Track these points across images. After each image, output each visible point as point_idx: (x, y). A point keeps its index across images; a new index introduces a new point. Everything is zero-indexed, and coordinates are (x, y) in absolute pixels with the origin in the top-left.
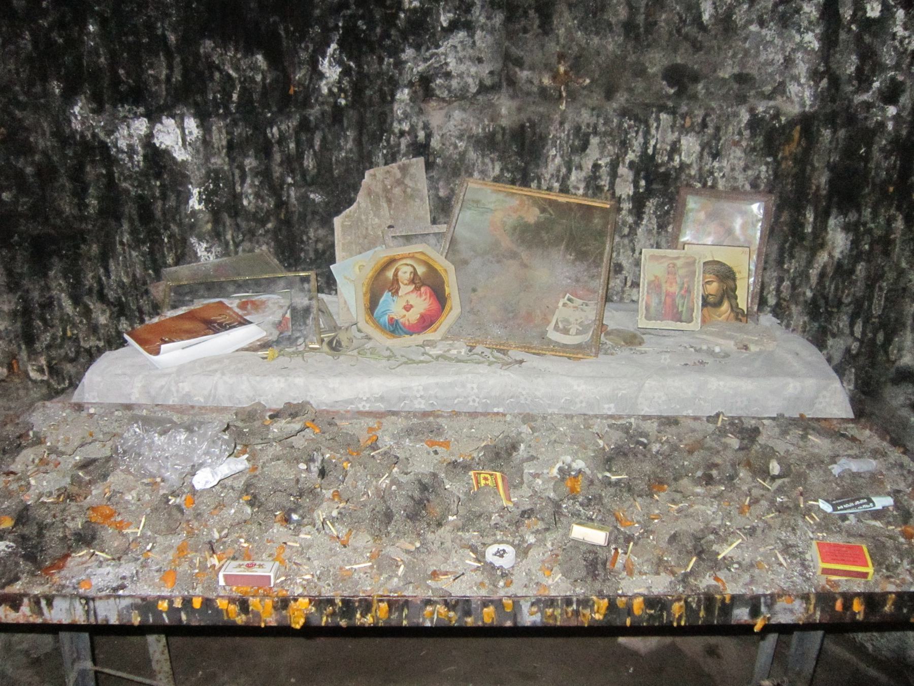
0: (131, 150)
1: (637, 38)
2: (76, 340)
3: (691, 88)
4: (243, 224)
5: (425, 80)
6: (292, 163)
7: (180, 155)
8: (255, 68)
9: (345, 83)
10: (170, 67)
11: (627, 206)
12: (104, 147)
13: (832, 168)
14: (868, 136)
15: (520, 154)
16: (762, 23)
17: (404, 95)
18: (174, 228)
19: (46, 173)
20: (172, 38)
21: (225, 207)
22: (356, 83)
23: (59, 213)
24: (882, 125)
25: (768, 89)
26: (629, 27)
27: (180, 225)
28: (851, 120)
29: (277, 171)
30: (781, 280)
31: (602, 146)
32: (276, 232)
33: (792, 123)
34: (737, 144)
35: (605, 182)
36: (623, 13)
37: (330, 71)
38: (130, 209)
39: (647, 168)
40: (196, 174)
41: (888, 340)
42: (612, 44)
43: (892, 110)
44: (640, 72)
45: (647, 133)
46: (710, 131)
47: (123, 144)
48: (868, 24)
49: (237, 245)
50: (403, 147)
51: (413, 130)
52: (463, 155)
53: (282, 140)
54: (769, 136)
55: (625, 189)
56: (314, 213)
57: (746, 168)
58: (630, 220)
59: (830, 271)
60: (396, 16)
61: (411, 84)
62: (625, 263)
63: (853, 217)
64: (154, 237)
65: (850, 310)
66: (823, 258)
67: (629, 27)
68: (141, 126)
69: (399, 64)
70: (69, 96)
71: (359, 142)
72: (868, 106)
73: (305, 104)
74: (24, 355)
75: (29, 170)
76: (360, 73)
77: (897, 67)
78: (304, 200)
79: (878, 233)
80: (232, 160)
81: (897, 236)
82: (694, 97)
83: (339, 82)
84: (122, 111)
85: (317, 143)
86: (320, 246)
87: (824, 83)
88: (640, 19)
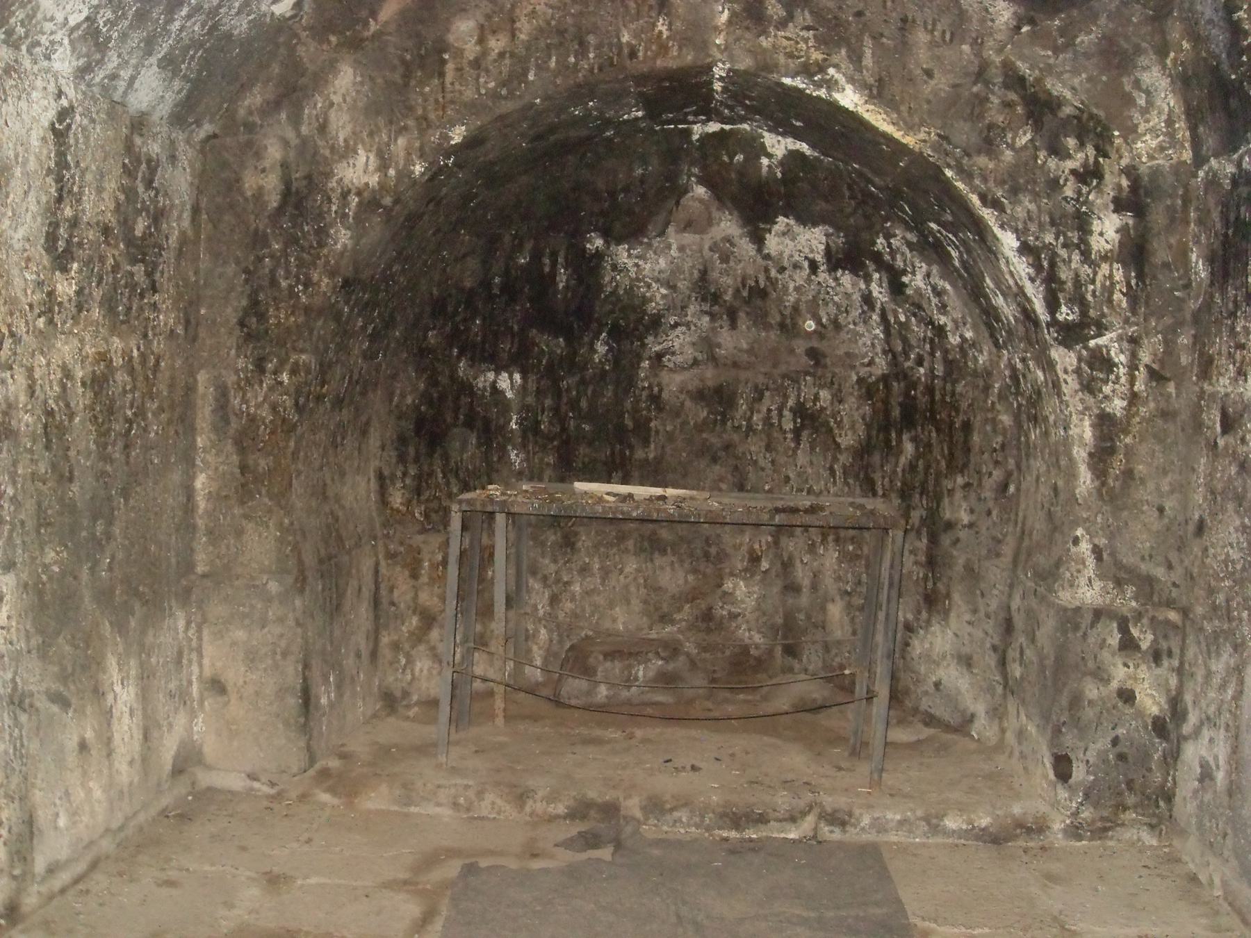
0: (485, 388)
1: (787, 331)
2: (439, 499)
3: (823, 361)
4: (540, 440)
5: (659, 356)
6: (574, 405)
7: (509, 395)
8: (558, 345)
9: (610, 356)
10: (512, 343)
11: (789, 436)
12: (471, 386)
13: (900, 404)
14: (913, 385)
15: (720, 403)
16: (855, 324)
17: (646, 364)
18: (500, 439)
19: (442, 398)
20: (516, 327)
21: (531, 429)
22: (616, 358)
23: (445, 421)
24: (919, 378)
25: (866, 360)
26: (782, 326)
27: (504, 437)
28: (906, 376)
29: (564, 408)
30: (883, 478)
31: (772, 396)
32: (558, 449)
33: (878, 381)
34: (852, 394)
35: (775, 421)
36: (778, 318)
37: (601, 348)
38: (479, 424)
39: (800, 410)
40: (515, 406)
41: (938, 506)
42: (773, 335)
43: (922, 370)
44: (792, 351)
45: (799, 389)
46: (836, 386)
47: (480, 385)
48: (900, 324)
49: (534, 454)
50: (644, 397)
51: (650, 387)
52: (683, 404)
53: (568, 390)
54: (868, 390)
55: (788, 425)
56: (584, 438)
57: (857, 409)
58: (793, 445)
59: (907, 468)
60: (643, 318)
61: (650, 358)
62: (791, 476)
63: (913, 433)
64: (488, 442)
65: (918, 490)
66: (903, 460)
67: (782, 326)
68: (491, 376)
69: (643, 345)
70: (459, 358)
71: (616, 394)
72: (912, 368)
73: (585, 368)
74: (415, 502)
75: (435, 395)
76: (619, 350)
77: (918, 347)
78: (578, 427)
79: (926, 440)
80: (538, 399)
81: (933, 441)
82: (825, 366)
83: (606, 355)
84: (483, 366)
85: (589, 392)
86: (586, 460)
87: (890, 356)
88: (788, 321)
